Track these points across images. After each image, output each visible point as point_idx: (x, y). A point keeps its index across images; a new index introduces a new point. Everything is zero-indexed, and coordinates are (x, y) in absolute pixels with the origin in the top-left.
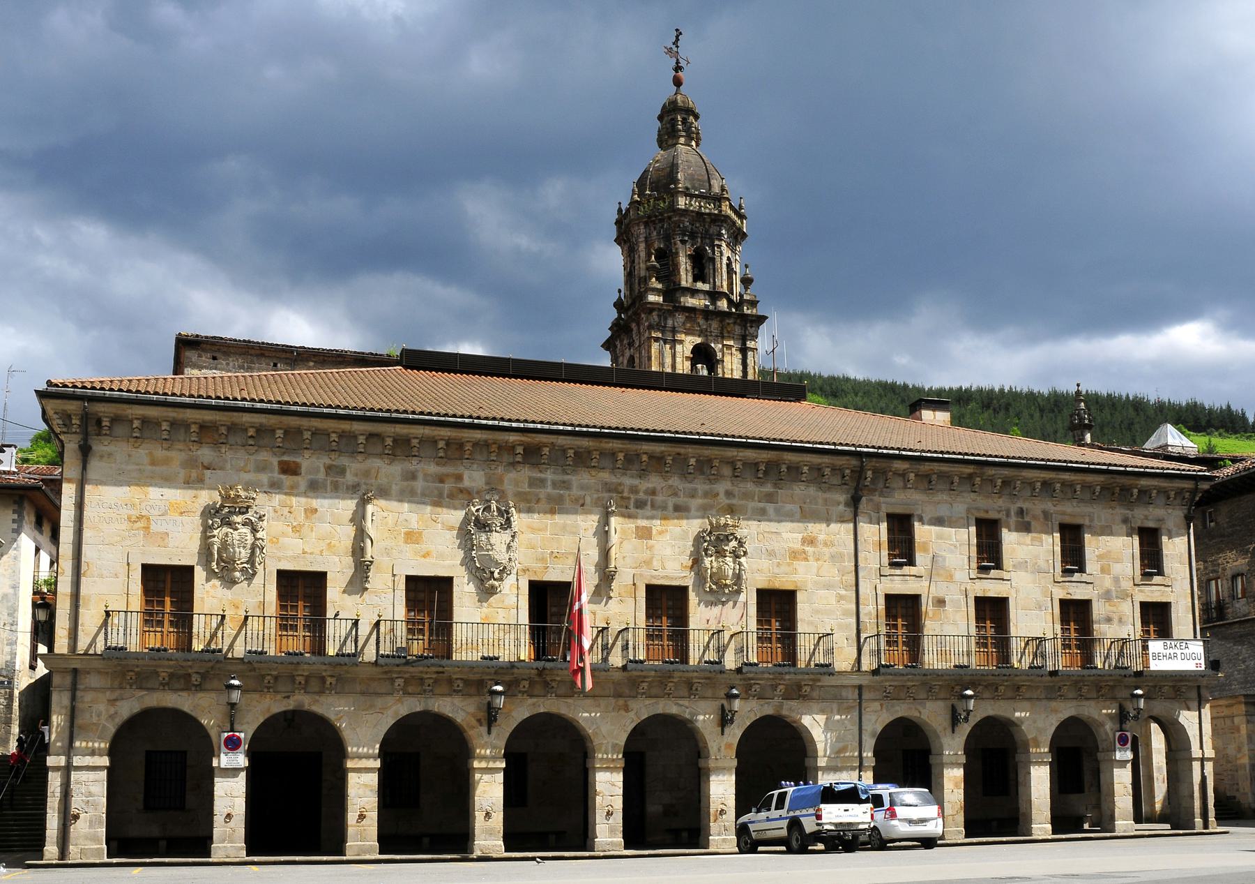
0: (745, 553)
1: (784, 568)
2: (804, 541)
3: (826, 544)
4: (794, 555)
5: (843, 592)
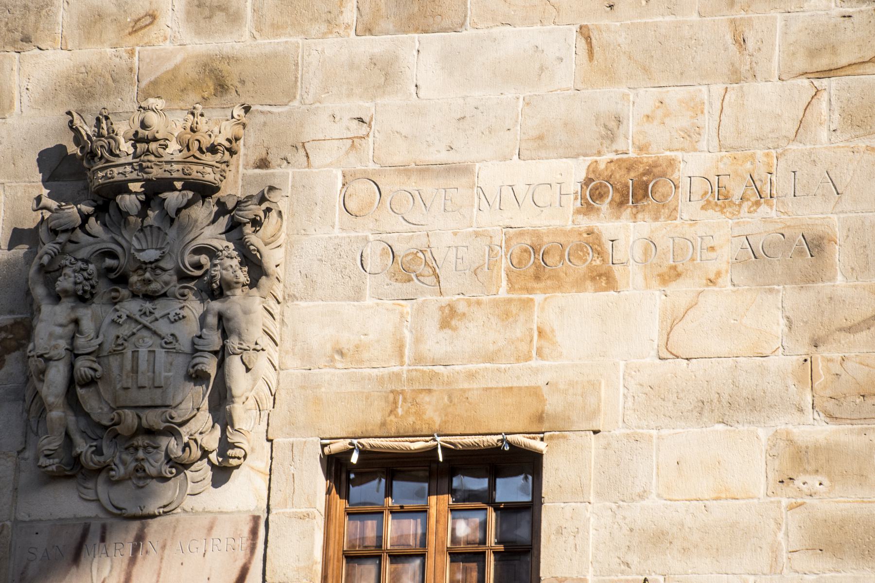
0: (256, 268)
1: (477, 332)
2: (594, 191)
3: (719, 197)
4: (538, 263)
5: (815, 430)
